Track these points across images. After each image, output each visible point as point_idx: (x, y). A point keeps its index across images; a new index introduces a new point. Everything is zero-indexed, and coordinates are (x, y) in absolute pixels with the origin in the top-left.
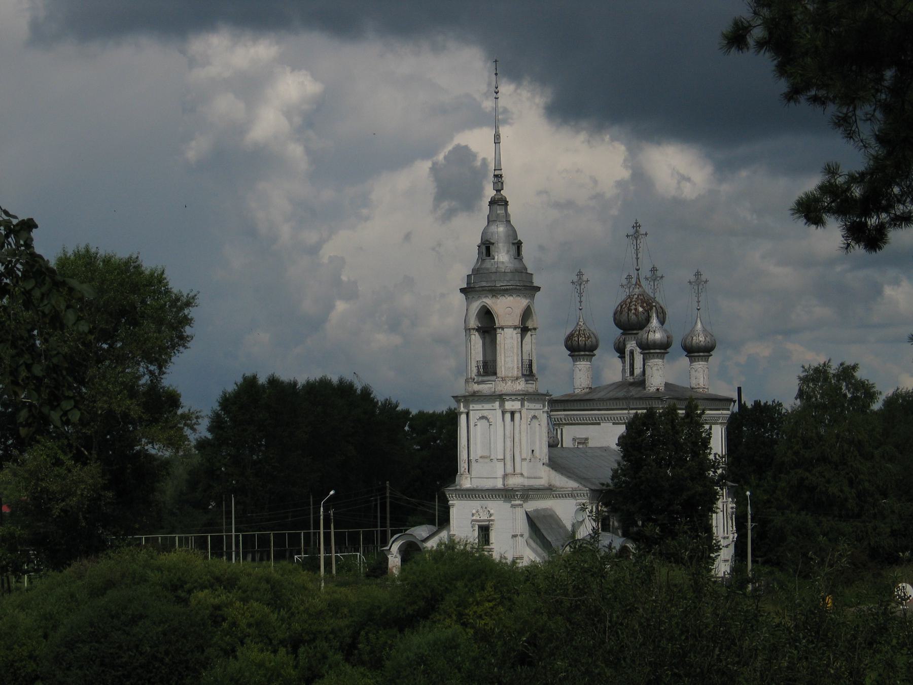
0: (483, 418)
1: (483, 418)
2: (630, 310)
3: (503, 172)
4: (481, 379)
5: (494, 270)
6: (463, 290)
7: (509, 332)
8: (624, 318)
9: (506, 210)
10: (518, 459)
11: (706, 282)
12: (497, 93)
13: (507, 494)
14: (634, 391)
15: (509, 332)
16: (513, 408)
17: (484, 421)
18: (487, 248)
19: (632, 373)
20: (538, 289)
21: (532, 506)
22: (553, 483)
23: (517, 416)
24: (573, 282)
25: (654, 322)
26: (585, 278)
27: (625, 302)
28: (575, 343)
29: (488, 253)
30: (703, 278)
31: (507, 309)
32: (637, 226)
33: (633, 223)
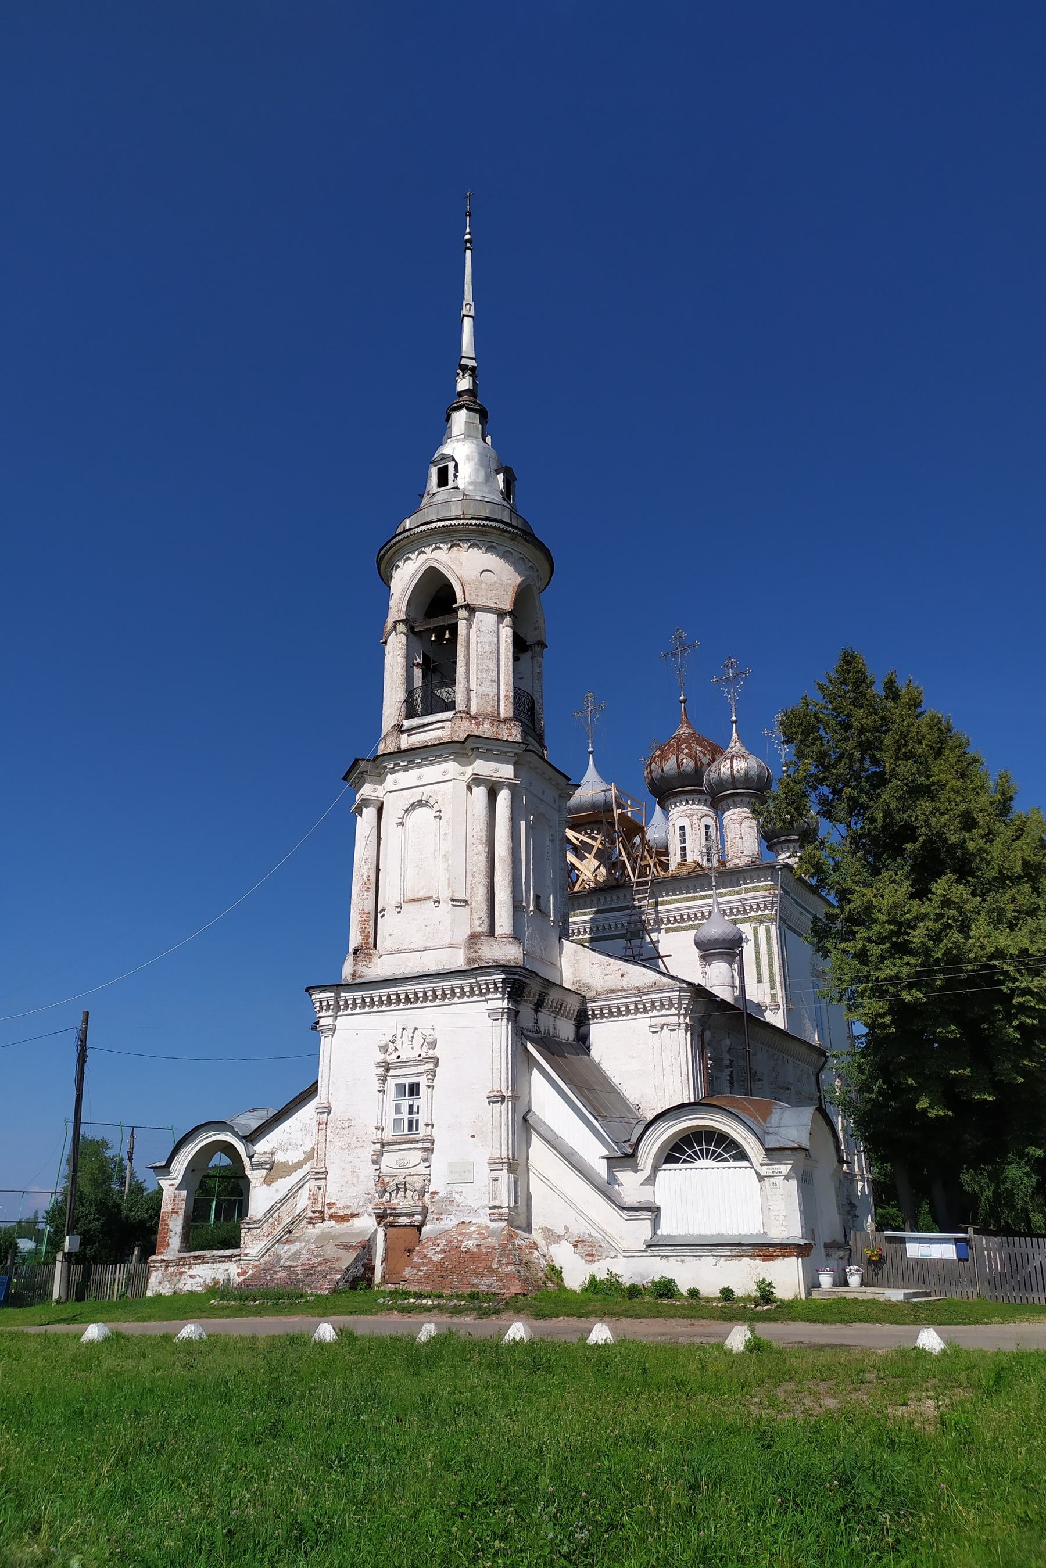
0: (420, 803)
1: (420, 803)
4: (415, 722)
7: (485, 621)
15: (485, 621)
17: (423, 814)
23: (504, 797)
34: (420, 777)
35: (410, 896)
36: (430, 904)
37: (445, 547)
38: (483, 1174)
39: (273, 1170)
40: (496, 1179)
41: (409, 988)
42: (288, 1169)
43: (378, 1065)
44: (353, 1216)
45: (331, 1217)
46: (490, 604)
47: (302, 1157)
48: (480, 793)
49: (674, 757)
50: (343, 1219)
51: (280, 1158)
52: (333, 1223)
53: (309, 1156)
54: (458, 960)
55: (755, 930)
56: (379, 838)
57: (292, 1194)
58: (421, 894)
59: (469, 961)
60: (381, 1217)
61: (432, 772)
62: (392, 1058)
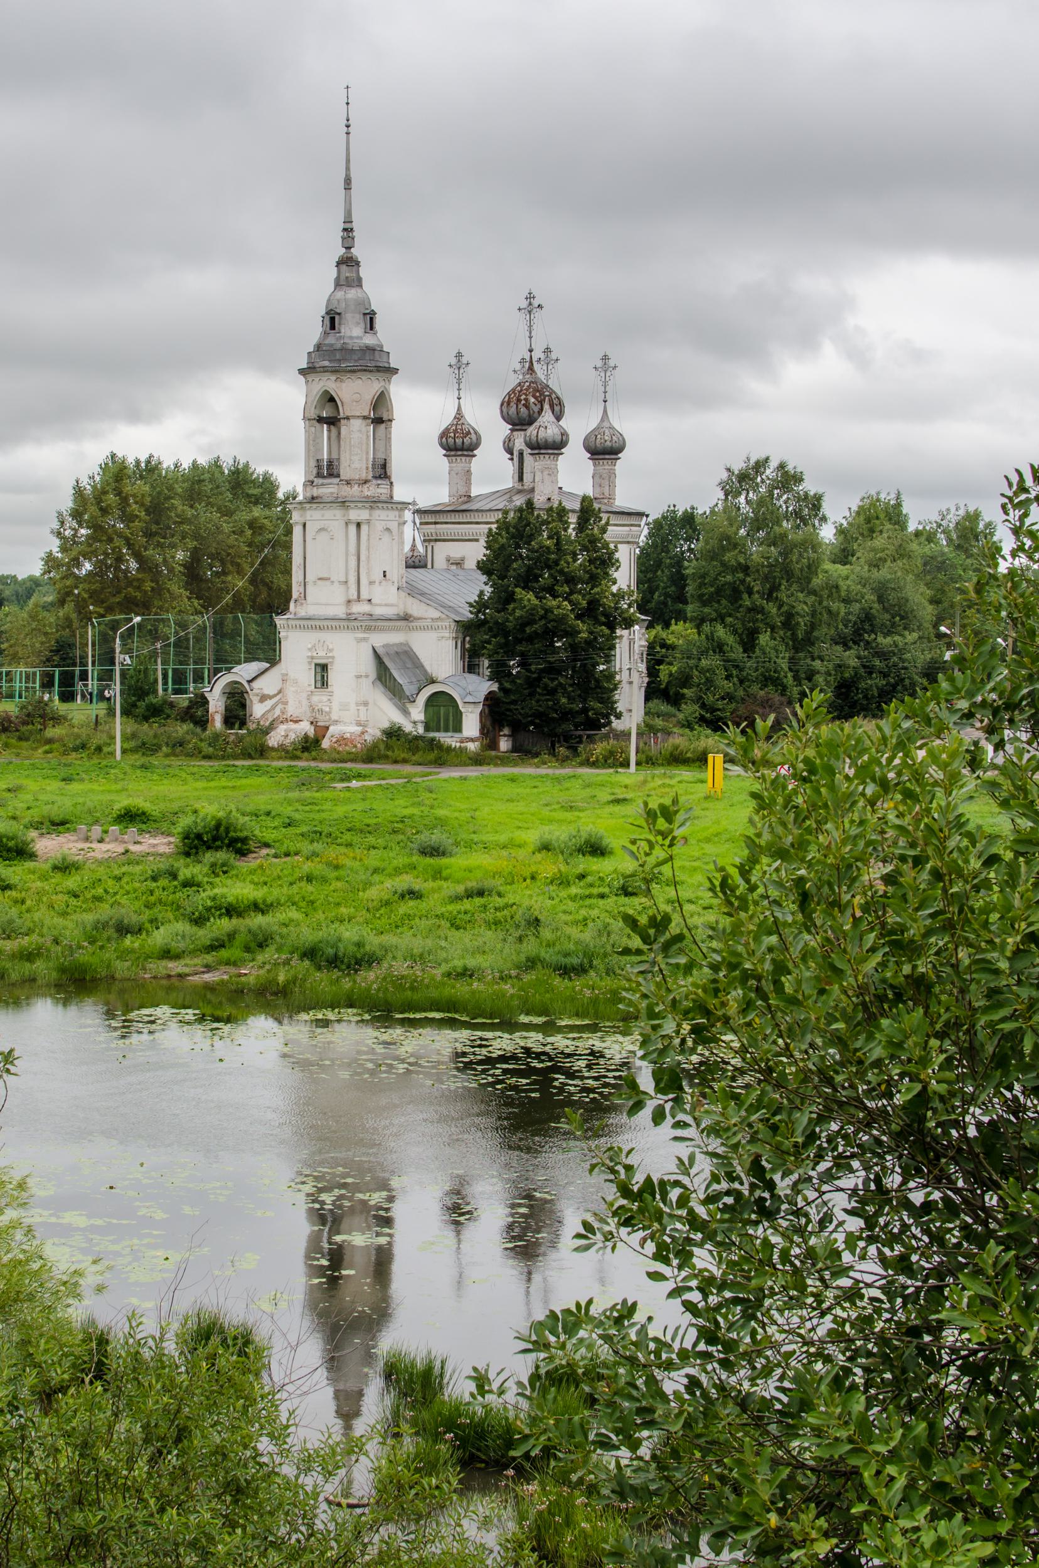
2: (519, 400)
3: (355, 225)
4: (321, 481)
5: (338, 346)
6: (302, 372)
7: (356, 424)
10: (364, 581)
13: (349, 621)
15: (356, 424)
16: (359, 519)
17: (323, 533)
18: (332, 320)
19: (521, 479)
20: (395, 371)
21: (380, 640)
22: (410, 612)
23: (364, 528)
25: (547, 417)
26: (464, 360)
27: (513, 390)
28: (451, 441)
29: (333, 327)
31: (356, 394)
33: (526, 294)
36: (328, 583)
37: (333, 378)
38: (353, 707)
39: (263, 698)
41: (321, 623)
48: (353, 529)
50: (296, 722)
51: (266, 692)
53: (280, 692)
57: (273, 708)
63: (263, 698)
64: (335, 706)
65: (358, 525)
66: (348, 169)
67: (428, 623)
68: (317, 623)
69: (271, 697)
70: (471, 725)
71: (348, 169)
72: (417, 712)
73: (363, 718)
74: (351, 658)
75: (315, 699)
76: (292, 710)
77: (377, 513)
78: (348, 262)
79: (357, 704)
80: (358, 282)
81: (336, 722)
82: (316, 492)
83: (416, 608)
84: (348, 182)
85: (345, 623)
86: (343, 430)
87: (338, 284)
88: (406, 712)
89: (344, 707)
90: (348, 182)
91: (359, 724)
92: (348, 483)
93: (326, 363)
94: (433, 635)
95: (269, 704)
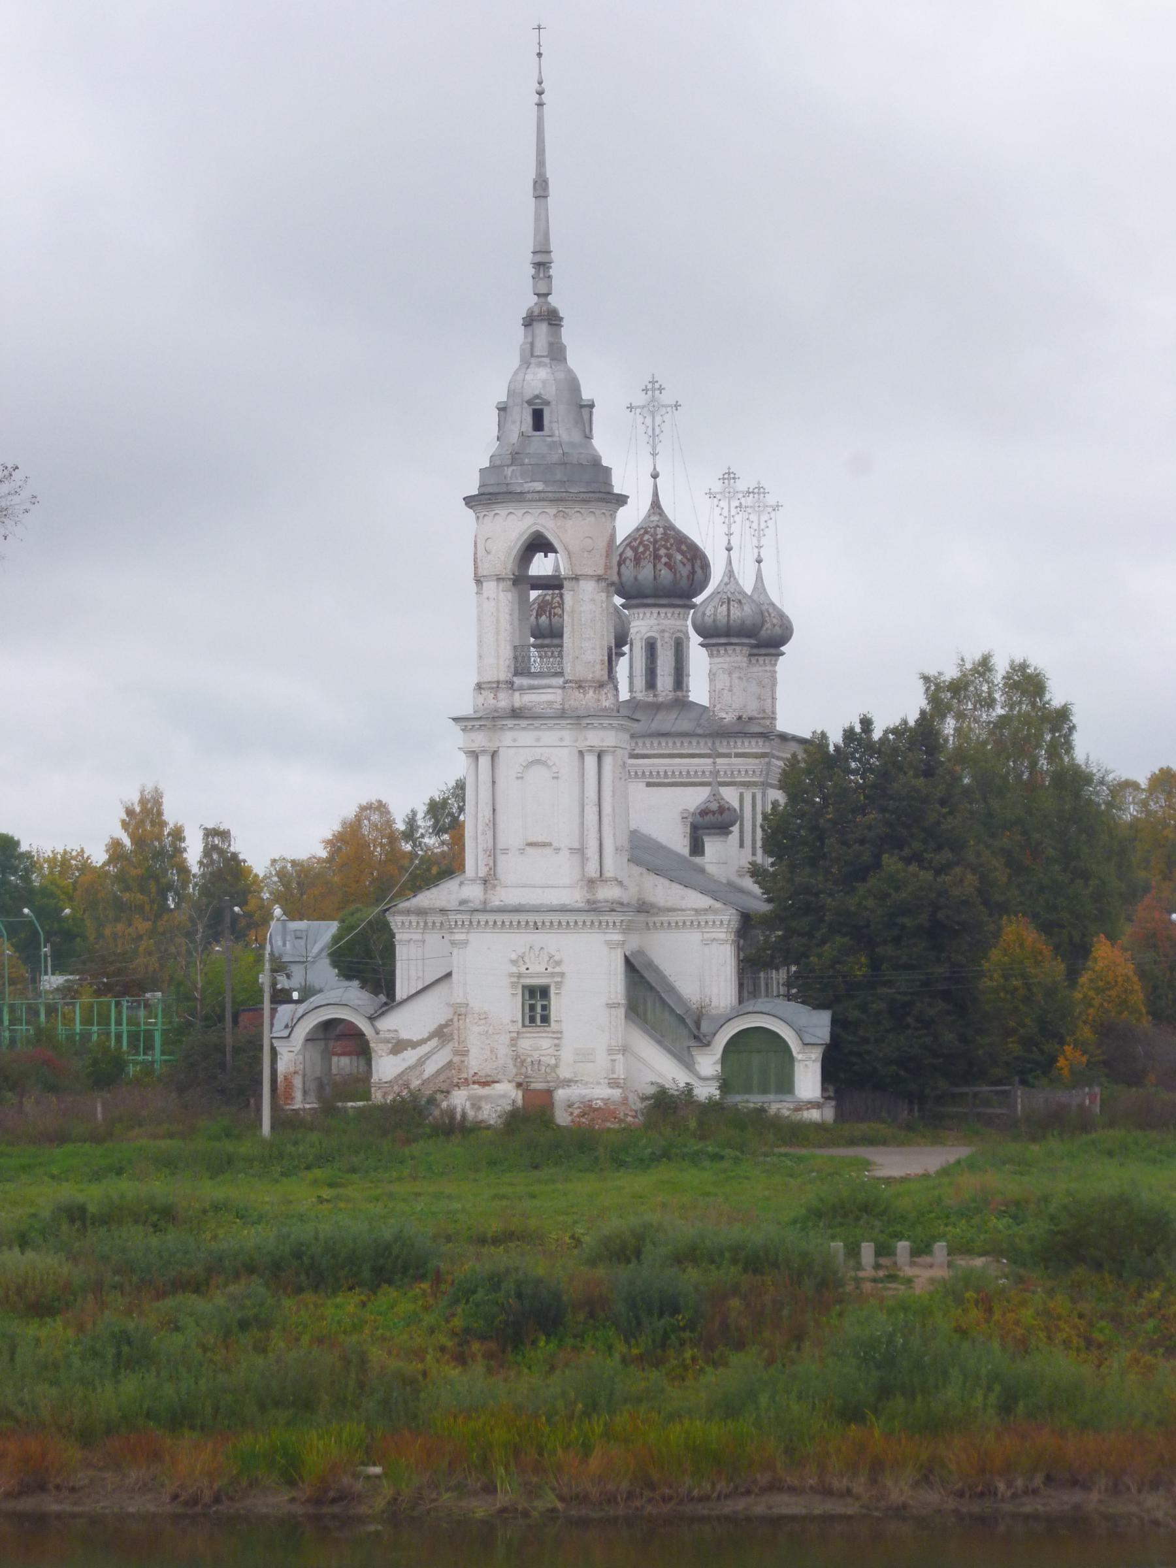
5: (555, 457)
6: (469, 501)
8: (646, 573)
9: (558, 335)
11: (776, 507)
12: (540, 93)
14: (667, 721)
17: (538, 772)
19: (651, 684)
22: (650, 898)
23: (608, 761)
24: (711, 495)
30: (771, 500)
32: (653, 387)
34: (538, 740)
35: (531, 840)
36: (548, 851)
39: (399, 1046)
40: (613, 1061)
41: (538, 918)
42: (414, 1045)
43: (511, 975)
44: (494, 1082)
45: (474, 1083)
46: (591, 573)
47: (426, 1035)
48: (591, 761)
49: (651, 566)
51: (405, 1035)
52: (476, 1086)
54: (574, 897)
55: (741, 795)
56: (494, 782)
57: (421, 1062)
58: (540, 839)
59: (588, 901)
60: (519, 1085)
61: (550, 737)
62: (523, 969)
63: (399, 1046)
64: (567, 1056)
65: (599, 757)
66: (541, 163)
67: (689, 917)
68: (531, 918)
69: (414, 1045)
70: (808, 1081)
71: (541, 163)
72: (709, 1063)
73: (620, 1073)
74: (590, 977)
75: (525, 1044)
76: (476, 1063)
77: (507, 738)
78: (545, 317)
79: (610, 1051)
80: (557, 353)
81: (568, 1083)
82: (519, 700)
83: (663, 892)
84: (541, 188)
85: (588, 918)
86: (568, 597)
87: (529, 357)
88: (688, 1064)
89: (585, 1056)
90: (541, 188)
91: (614, 1084)
92: (580, 685)
93: (539, 486)
94: (695, 936)
95: (410, 1057)
